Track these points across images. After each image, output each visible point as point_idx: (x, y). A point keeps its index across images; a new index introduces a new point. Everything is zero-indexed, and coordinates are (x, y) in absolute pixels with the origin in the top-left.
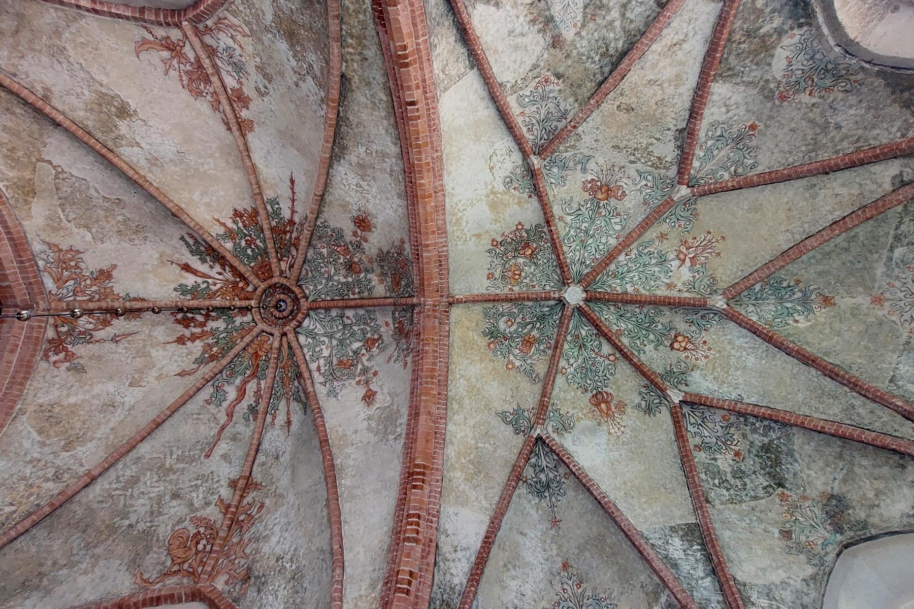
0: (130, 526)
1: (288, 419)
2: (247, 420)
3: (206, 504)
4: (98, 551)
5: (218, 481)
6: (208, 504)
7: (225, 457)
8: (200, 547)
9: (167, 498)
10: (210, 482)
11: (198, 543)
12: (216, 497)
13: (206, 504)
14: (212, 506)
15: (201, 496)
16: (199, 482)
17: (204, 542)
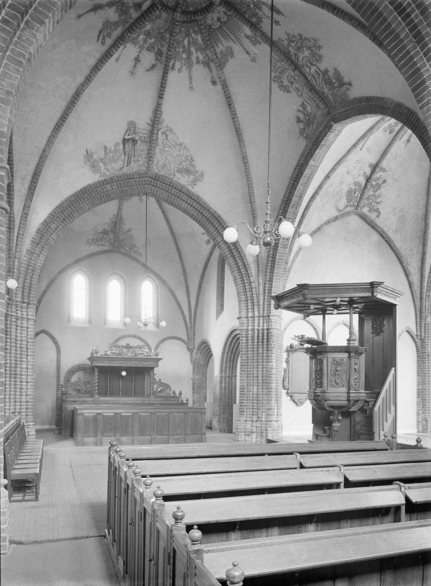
0: (334, 190)
1: (409, 138)
2: (385, 130)
3: (359, 175)
4: (324, 201)
5: (364, 163)
6: (359, 175)
7: (369, 150)
8: (356, 195)
9: (345, 174)
10: (361, 163)
11: (355, 193)
12: (363, 172)
13: (359, 175)
14: (361, 176)
15: (357, 171)
16: (357, 164)
17: (357, 193)
